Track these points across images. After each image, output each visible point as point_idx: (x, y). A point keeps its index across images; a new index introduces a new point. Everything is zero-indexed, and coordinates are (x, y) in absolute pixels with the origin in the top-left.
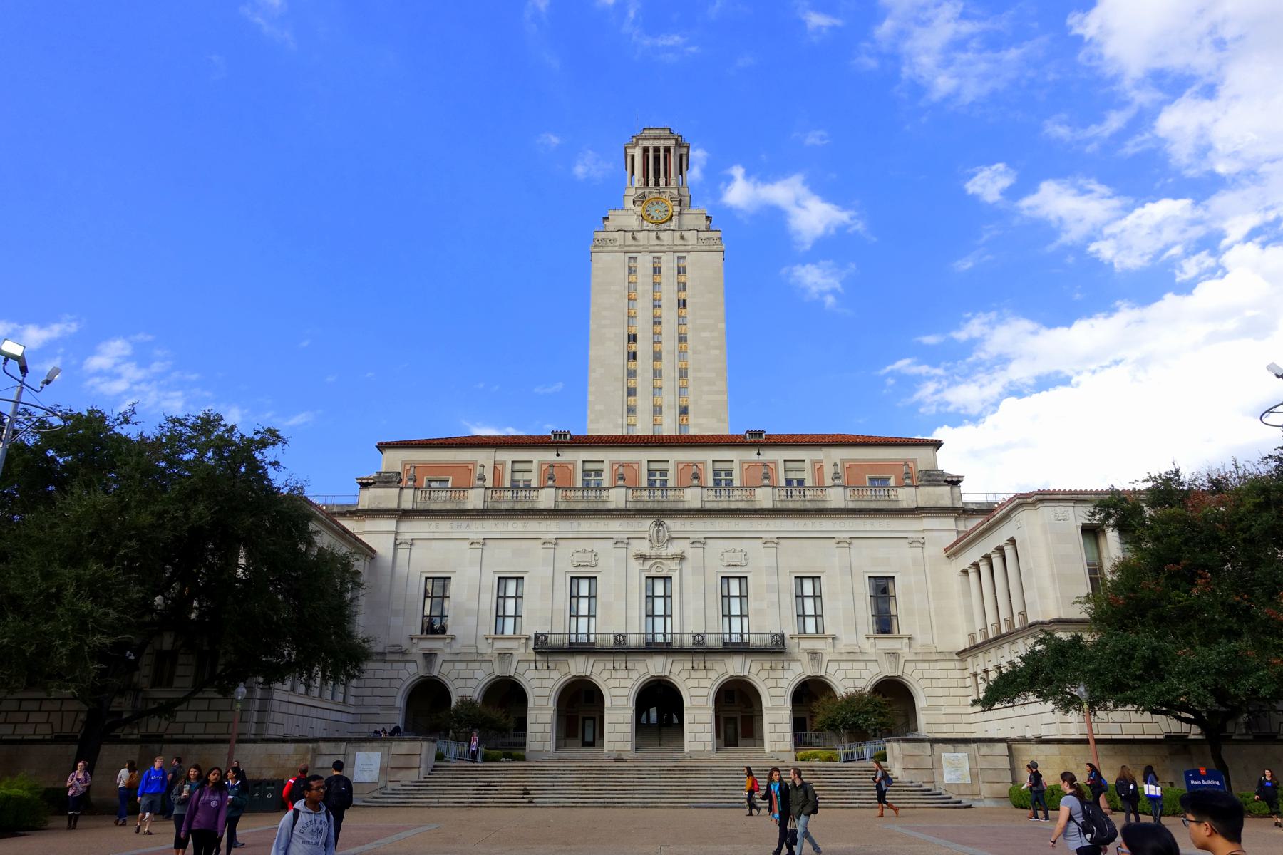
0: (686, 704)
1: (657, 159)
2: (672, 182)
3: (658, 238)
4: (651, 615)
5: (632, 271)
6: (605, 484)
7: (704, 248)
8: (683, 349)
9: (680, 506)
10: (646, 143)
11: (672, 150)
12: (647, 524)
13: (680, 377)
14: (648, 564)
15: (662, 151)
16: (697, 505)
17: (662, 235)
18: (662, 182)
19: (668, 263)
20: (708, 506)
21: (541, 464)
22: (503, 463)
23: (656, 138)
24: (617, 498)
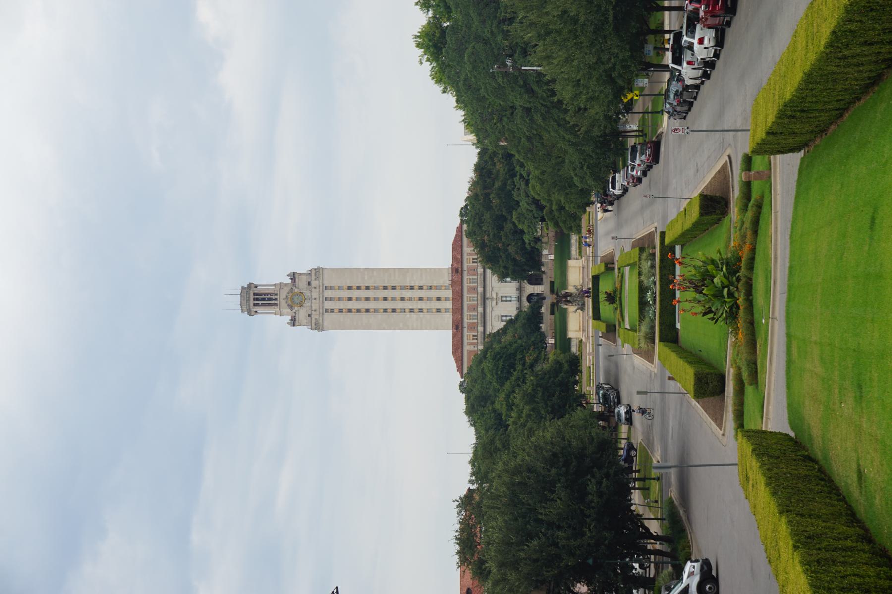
0: (531, 292)
1: (257, 299)
2: (275, 292)
3: (315, 299)
4: (511, 301)
5: (332, 311)
6: (476, 314)
7: (321, 277)
8: (373, 287)
9: (482, 293)
10: (252, 305)
11: (256, 292)
12: (488, 302)
13: (386, 289)
14: (498, 302)
15: (256, 297)
16: (482, 289)
17: (313, 297)
18: (276, 297)
19: (328, 293)
20: (482, 286)
21: (468, 332)
22: (468, 343)
23: (248, 301)
24: (480, 310)
